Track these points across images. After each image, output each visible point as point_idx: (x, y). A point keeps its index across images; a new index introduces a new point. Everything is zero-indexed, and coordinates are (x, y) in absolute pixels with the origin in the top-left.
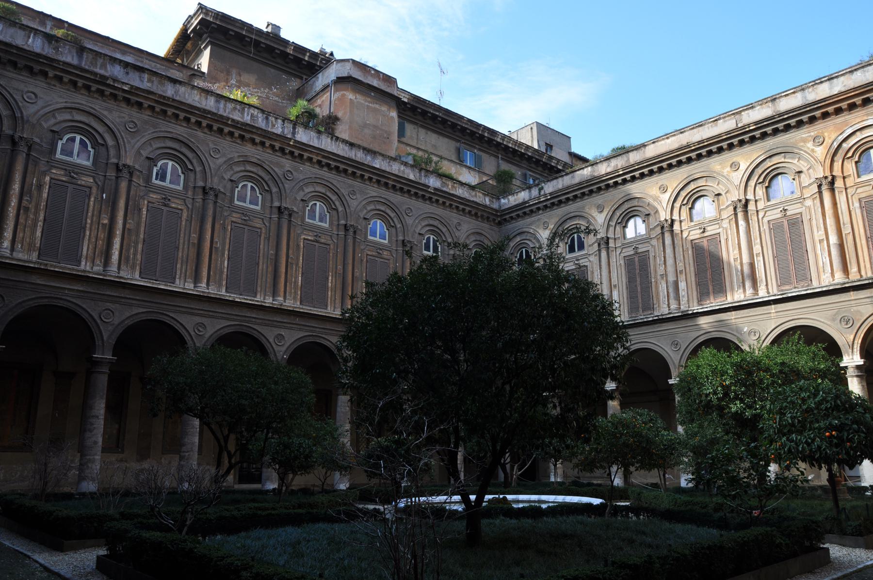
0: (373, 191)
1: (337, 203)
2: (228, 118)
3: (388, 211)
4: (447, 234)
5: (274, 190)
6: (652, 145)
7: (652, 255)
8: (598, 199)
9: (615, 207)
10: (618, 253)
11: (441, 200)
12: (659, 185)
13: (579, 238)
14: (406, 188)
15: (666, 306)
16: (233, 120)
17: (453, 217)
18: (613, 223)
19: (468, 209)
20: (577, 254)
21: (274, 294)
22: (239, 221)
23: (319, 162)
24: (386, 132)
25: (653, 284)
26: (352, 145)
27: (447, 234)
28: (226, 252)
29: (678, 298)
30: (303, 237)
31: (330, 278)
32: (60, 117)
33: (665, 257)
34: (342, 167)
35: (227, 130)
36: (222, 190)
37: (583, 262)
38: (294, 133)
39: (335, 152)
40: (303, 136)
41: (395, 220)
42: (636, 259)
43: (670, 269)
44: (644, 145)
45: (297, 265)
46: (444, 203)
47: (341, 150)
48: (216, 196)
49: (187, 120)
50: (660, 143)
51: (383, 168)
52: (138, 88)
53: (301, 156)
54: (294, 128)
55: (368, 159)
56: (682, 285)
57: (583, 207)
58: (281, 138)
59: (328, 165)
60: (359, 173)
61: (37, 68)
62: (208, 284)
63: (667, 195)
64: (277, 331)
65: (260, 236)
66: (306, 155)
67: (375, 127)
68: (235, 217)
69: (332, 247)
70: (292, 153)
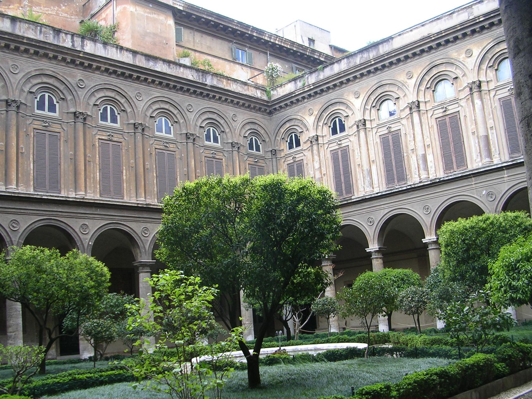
0: (157, 93)
1: (126, 105)
2: (23, 37)
3: (172, 109)
4: (225, 125)
5: (69, 97)
6: (399, 38)
7: (403, 132)
8: (354, 87)
9: (370, 92)
10: (374, 133)
11: (218, 96)
12: (406, 72)
13: (340, 121)
14: (186, 88)
15: (417, 176)
16: (28, 39)
17: (228, 111)
18: (369, 107)
19: (242, 102)
20: (339, 135)
21: (76, 189)
22: (41, 127)
24: (165, 38)
25: (406, 158)
26: (135, 53)
27: (225, 125)
28: (31, 156)
29: (426, 169)
30: (98, 137)
31: (124, 171)
33: (414, 134)
35: (22, 48)
36: (23, 101)
37: (344, 143)
38: (83, 46)
39: (121, 60)
40: (89, 47)
41: (178, 116)
42: (390, 138)
43: (419, 144)
44: (391, 38)
45: (94, 162)
46: (220, 98)
47: (126, 58)
48: (18, 107)
50: (405, 35)
51: (164, 71)
53: (90, 66)
54: (83, 42)
55: (151, 65)
56: (430, 158)
57: (342, 95)
58: (72, 51)
62: (17, 185)
63: (413, 81)
64: (82, 222)
65: (60, 140)
66: (95, 65)
67: (155, 34)
68: (37, 124)
69: (124, 143)
70: (82, 64)
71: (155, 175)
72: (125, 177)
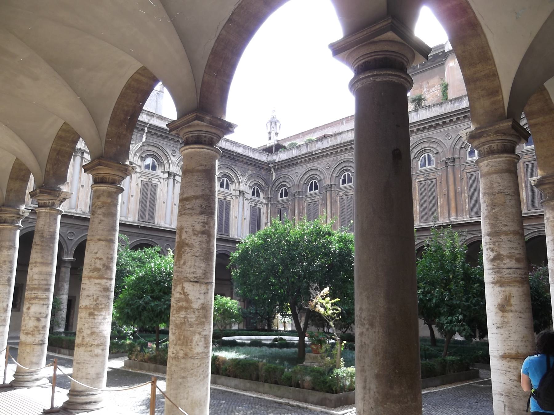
23: (418, 130)
30: (417, 180)
31: (439, 200)
32: (306, 177)
34: (433, 124)
49: (346, 149)
52: (323, 149)
59: (424, 128)
60: (447, 120)
61: (295, 162)
71: (466, 195)
72: (439, 204)
